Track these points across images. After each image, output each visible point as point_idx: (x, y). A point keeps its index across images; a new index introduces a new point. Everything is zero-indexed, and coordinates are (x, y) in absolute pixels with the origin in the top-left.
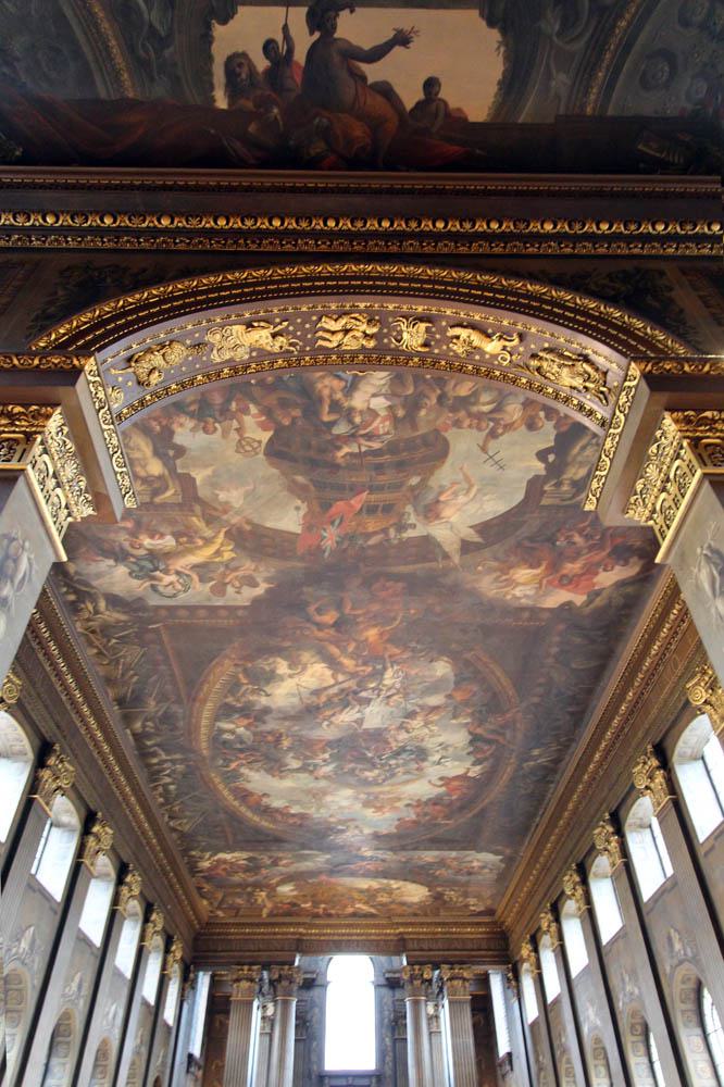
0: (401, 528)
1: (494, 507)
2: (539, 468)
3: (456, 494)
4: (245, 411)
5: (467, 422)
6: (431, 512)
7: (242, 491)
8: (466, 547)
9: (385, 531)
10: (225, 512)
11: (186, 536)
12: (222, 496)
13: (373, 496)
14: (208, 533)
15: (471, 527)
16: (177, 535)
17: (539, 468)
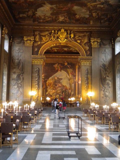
0: (56, 6)
1: (42, 9)
2: (36, 13)
3: (48, 10)
4: (78, 18)
5: (49, 16)
6: (51, 8)
7: (82, 11)
8: (45, 4)
9: (59, 6)
10: (86, 9)
11: (95, 6)
12: (86, 11)
13: (61, 10)
14: (90, 7)
15: (44, 6)
16: (97, 6)
17: (36, 13)
